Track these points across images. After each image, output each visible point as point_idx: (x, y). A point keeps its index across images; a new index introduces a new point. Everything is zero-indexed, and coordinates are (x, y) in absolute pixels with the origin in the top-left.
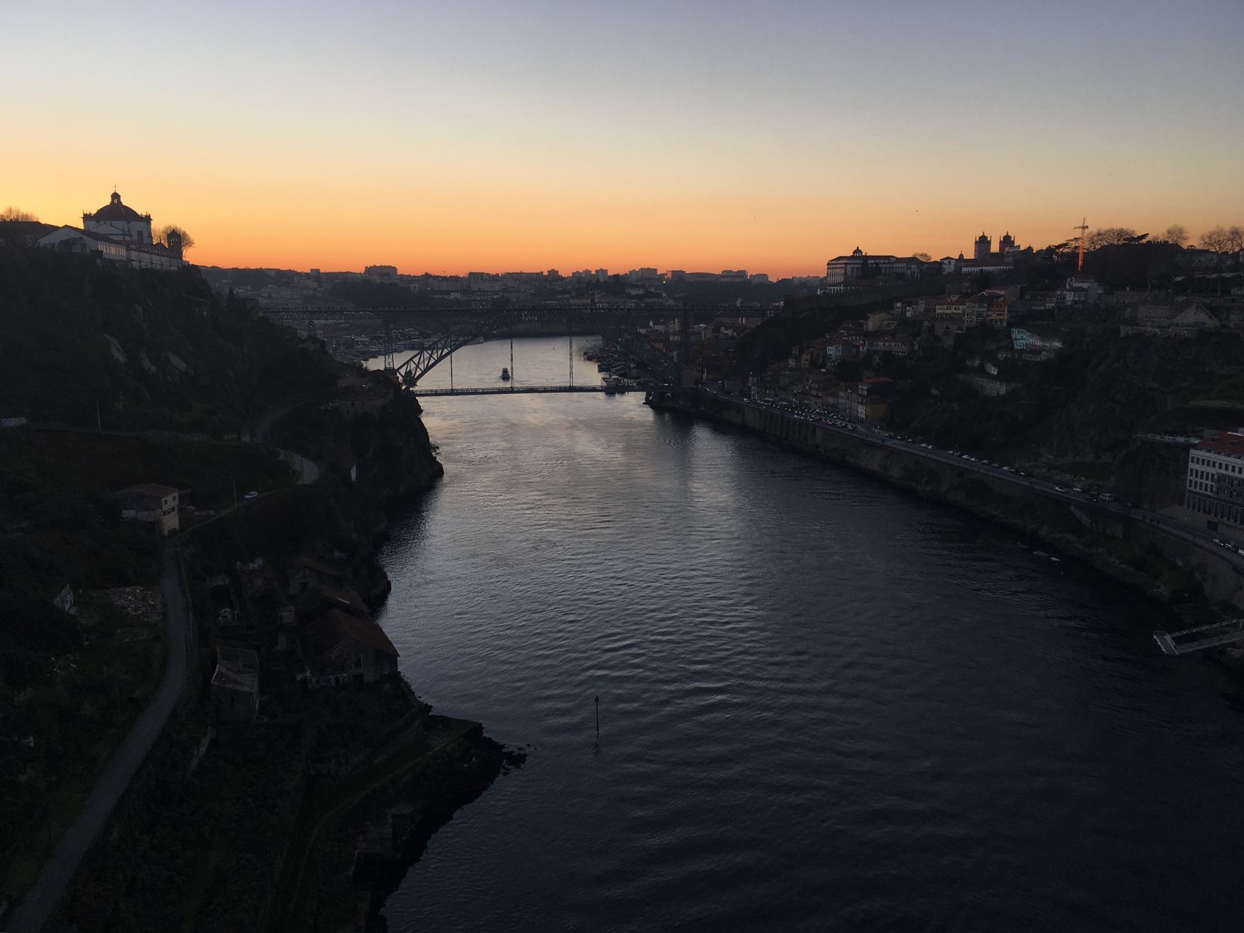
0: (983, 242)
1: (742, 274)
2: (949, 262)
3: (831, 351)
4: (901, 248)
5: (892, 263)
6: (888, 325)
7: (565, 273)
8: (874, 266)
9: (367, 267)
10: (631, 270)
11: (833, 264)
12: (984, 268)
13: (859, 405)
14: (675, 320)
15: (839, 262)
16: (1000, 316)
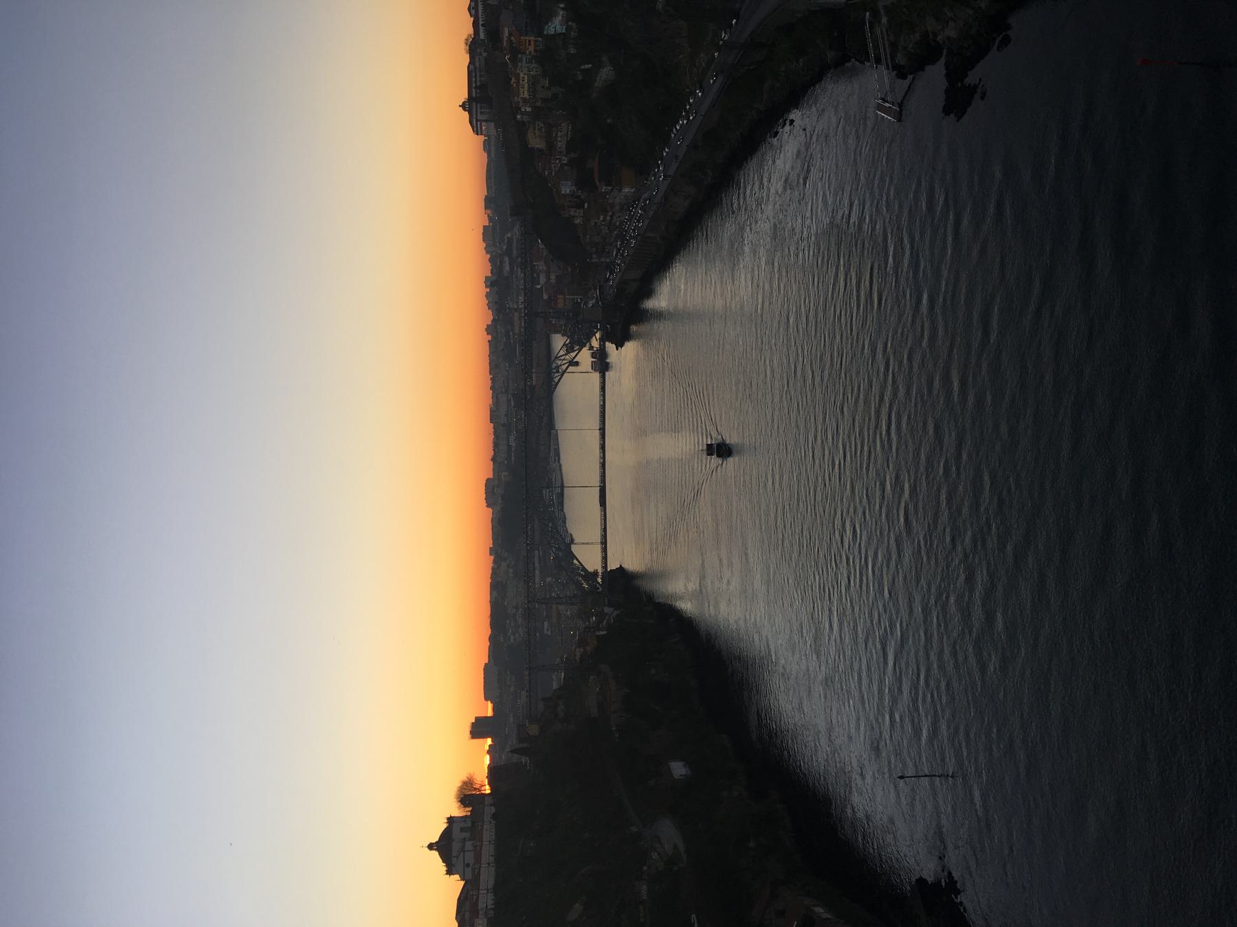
4: (463, 59)
5: (475, 68)
6: (540, 129)
7: (488, 317)
8: (478, 91)
9: (487, 506)
11: (477, 131)
13: (624, 190)
14: (534, 265)
16: (531, 44)
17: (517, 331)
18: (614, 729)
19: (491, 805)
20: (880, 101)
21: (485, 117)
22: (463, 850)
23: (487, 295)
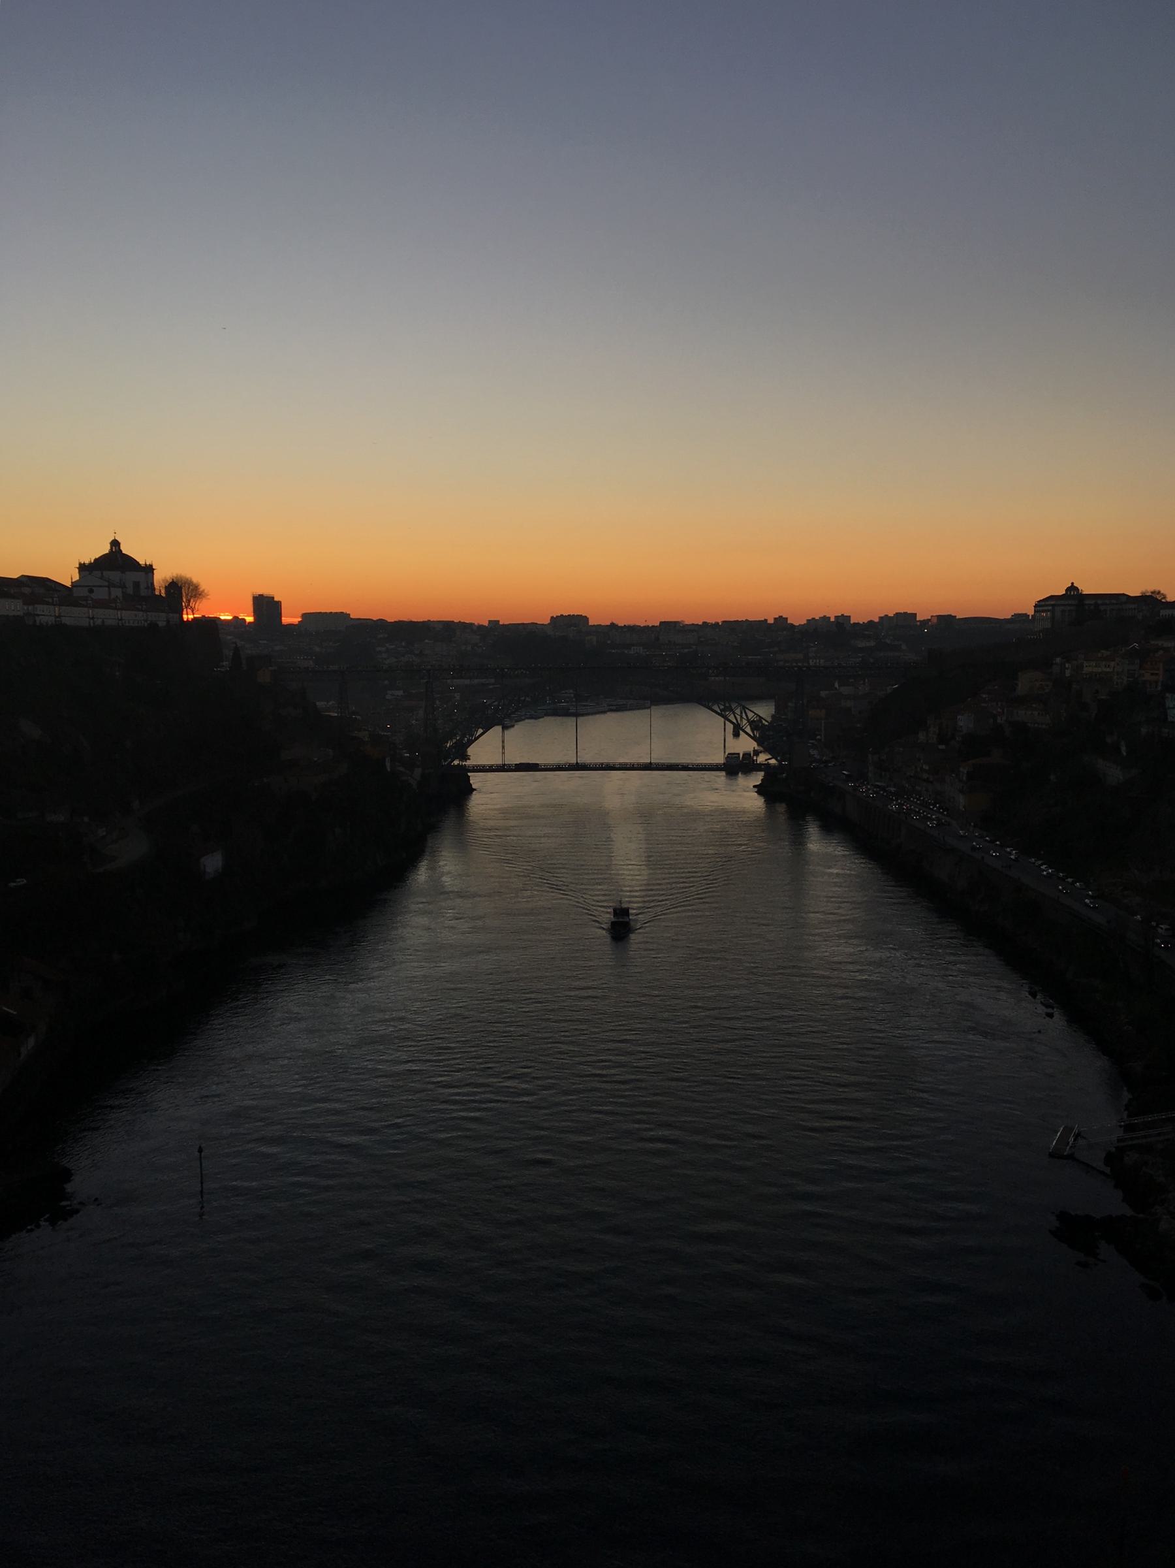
8: (1092, 607)
9: (552, 617)
10: (883, 615)
11: (1040, 605)
14: (864, 681)
15: (1047, 603)
19: (168, 621)
20: (1076, 1130)
22: (111, 585)
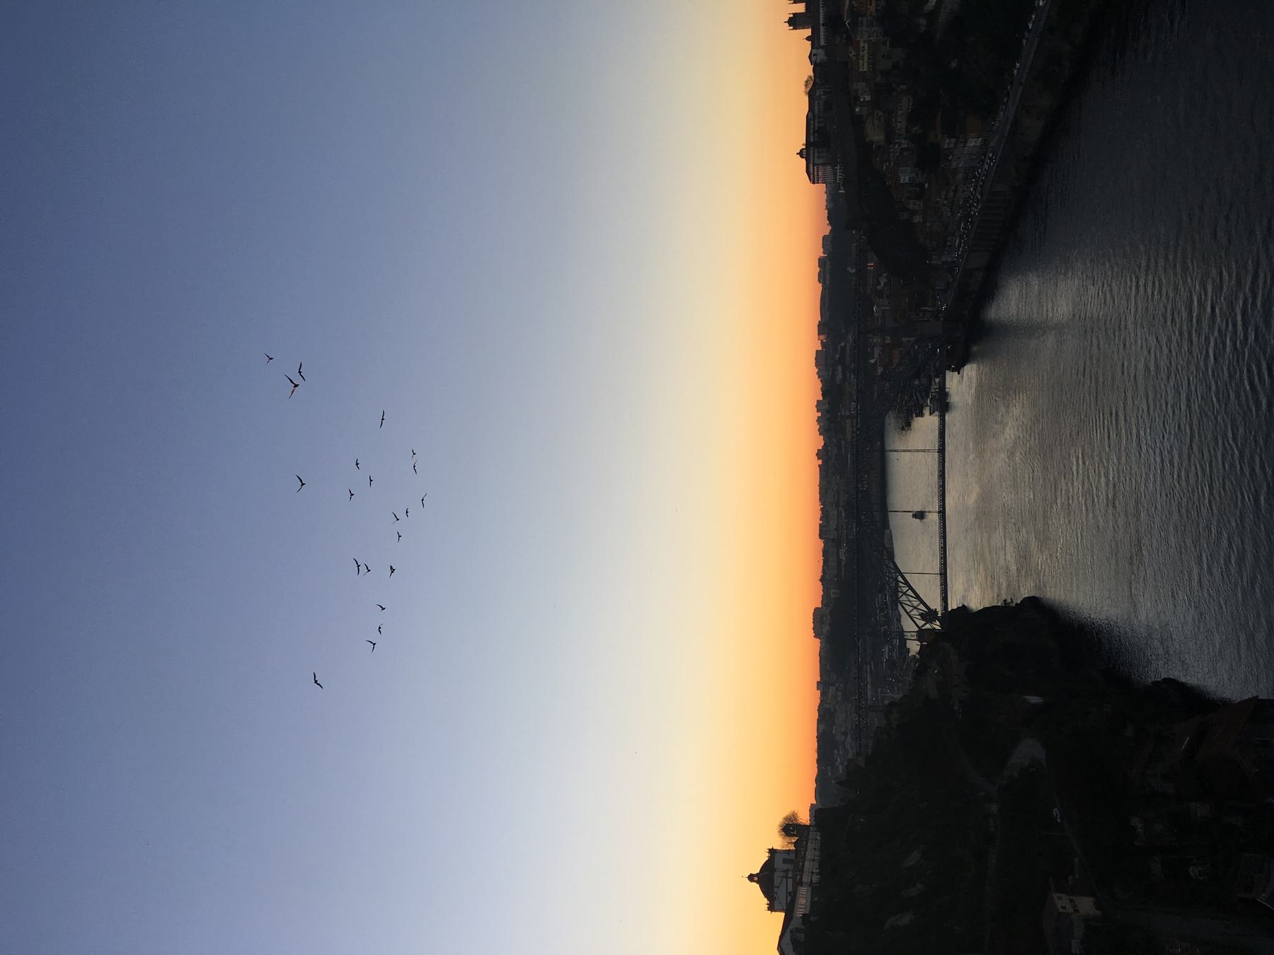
0: (795, 22)
1: (822, 262)
2: (814, 55)
3: (905, 179)
4: (801, 106)
5: (814, 116)
8: (816, 135)
11: (813, 180)
12: (821, 22)
13: (968, 145)
17: (849, 437)
18: (956, 708)
21: (820, 161)
23: (819, 420)
